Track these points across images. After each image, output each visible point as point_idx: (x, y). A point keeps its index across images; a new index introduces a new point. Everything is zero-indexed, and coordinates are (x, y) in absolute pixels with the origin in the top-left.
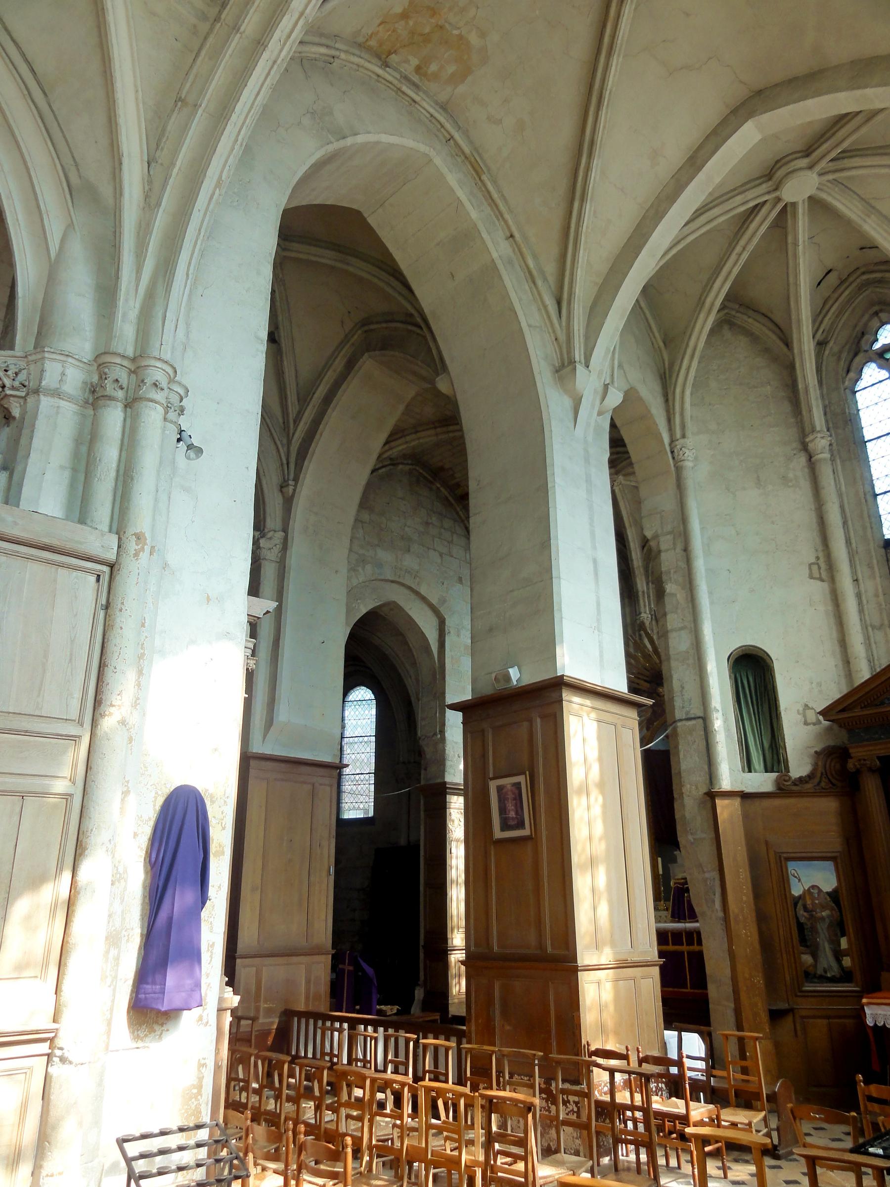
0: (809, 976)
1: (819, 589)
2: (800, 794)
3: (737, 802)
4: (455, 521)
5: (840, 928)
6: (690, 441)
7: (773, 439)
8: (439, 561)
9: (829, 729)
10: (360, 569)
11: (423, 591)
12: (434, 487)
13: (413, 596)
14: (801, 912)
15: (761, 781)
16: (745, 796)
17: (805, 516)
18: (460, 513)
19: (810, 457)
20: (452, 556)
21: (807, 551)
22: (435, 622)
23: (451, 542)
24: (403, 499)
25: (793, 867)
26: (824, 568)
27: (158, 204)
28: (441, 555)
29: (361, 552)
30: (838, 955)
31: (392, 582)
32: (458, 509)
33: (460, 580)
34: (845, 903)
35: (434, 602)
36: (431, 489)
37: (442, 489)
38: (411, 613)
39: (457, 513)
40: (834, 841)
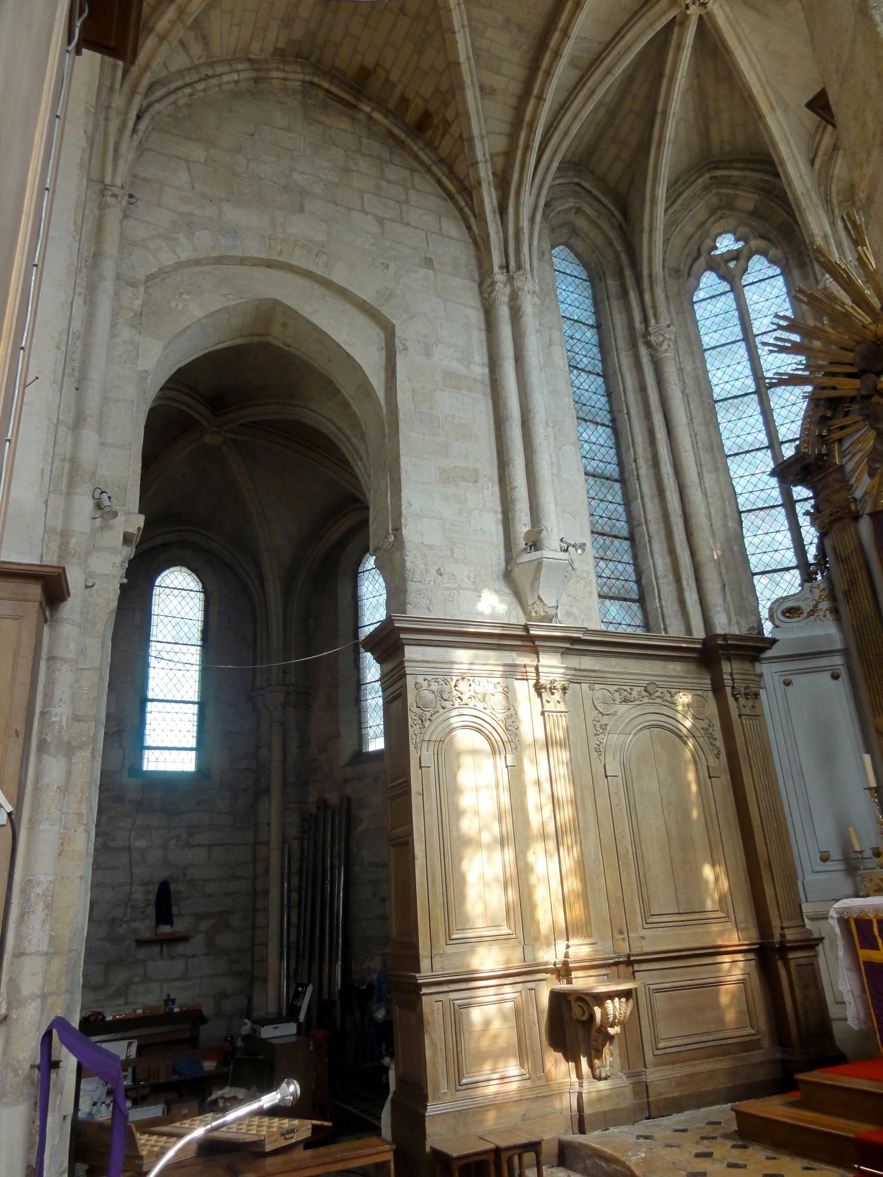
4: (413, 170)
8: (376, 229)
10: (182, 238)
11: (338, 277)
12: (361, 116)
13: (318, 290)
18: (421, 154)
20: (407, 224)
22: (376, 334)
23: (407, 201)
24: (288, 130)
28: (381, 221)
29: (184, 209)
31: (269, 264)
32: (415, 148)
33: (428, 263)
35: (367, 295)
36: (354, 119)
37: (376, 115)
38: (314, 320)
39: (416, 158)
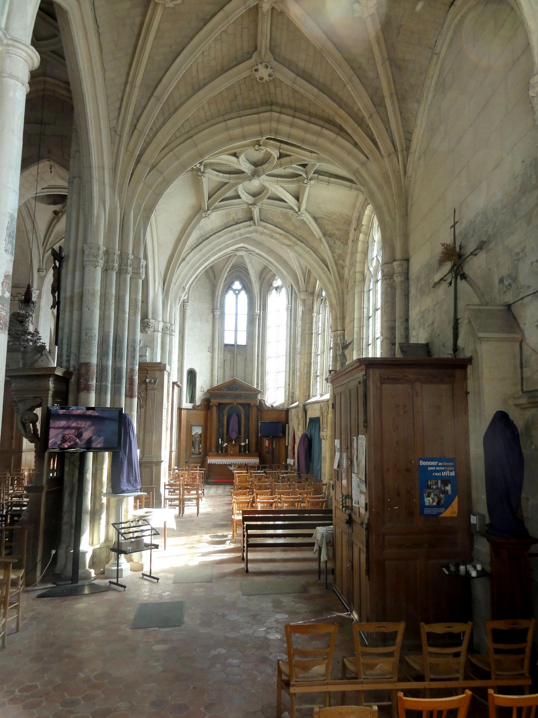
0: (193, 454)
1: (209, 354)
2: (198, 410)
3: (186, 411)
5: (200, 442)
6: (189, 304)
7: (206, 307)
9: (205, 393)
14: (194, 439)
15: (190, 406)
16: (188, 409)
17: (209, 333)
19: (214, 316)
21: (208, 344)
25: (194, 428)
26: (212, 350)
27: (176, 283)
30: (199, 449)
34: (202, 436)
40: (202, 422)
